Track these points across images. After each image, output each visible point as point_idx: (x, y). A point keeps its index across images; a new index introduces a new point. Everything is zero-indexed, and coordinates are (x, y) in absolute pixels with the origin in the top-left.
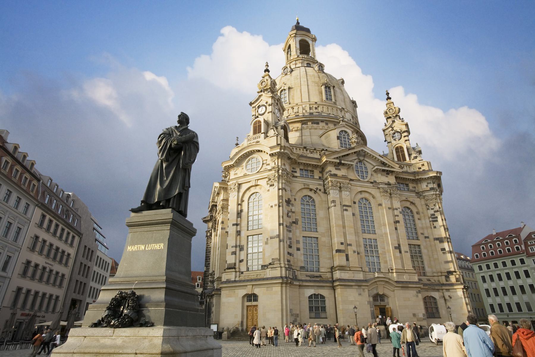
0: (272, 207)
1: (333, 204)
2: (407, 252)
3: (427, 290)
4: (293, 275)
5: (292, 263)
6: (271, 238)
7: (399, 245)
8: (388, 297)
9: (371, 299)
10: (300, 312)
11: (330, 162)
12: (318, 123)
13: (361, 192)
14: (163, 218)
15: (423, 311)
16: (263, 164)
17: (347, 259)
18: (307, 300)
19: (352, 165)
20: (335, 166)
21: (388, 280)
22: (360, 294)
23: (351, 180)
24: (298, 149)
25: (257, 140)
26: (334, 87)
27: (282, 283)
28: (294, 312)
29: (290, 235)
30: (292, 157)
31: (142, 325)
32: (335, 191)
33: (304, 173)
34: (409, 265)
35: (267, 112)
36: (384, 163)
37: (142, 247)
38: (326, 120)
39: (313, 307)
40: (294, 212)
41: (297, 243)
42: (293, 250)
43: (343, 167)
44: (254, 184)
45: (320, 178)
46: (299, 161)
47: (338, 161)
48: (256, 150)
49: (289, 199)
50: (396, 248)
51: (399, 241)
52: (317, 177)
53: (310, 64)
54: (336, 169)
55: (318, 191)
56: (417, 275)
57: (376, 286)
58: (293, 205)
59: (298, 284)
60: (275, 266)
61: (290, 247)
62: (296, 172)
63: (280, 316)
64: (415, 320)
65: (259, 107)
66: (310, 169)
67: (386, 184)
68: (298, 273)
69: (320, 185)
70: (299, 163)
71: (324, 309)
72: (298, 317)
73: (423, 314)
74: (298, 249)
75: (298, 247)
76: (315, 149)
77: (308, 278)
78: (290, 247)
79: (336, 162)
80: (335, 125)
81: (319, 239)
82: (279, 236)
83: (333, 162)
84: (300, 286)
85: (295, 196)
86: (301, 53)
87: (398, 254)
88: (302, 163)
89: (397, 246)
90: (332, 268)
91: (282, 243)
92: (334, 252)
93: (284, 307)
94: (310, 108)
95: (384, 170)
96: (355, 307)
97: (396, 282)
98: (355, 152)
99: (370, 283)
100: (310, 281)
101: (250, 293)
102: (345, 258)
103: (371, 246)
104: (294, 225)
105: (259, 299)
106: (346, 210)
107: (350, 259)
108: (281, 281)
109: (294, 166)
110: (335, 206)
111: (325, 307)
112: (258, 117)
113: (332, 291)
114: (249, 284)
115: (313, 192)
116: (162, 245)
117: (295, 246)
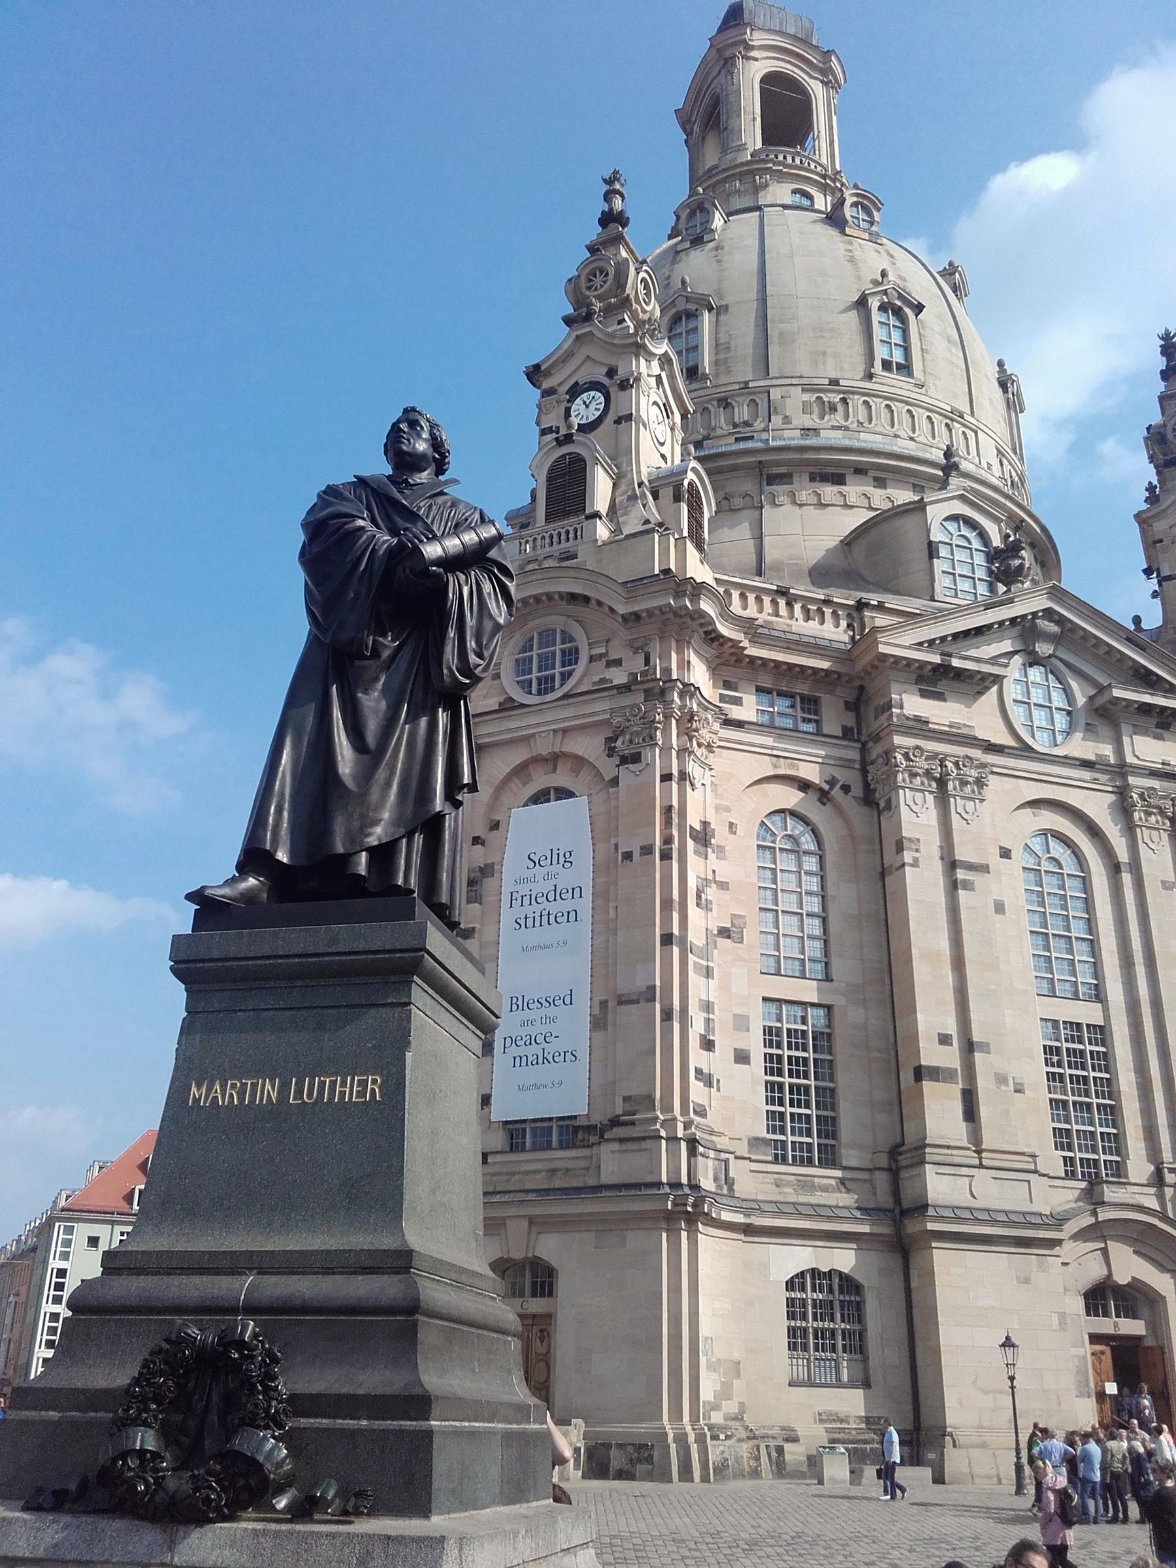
0: (628, 856)
1: (908, 857)
4: (716, 1179)
6: (622, 1001)
9: (1079, 1304)
11: (898, 660)
12: (839, 480)
13: (1035, 804)
16: (592, 659)
17: (971, 1113)
19: (998, 679)
20: (919, 680)
22: (1027, 1281)
23: (992, 748)
24: (751, 597)
25: (564, 545)
26: (919, 308)
30: (724, 629)
32: (919, 795)
33: (781, 705)
35: (611, 417)
36: (1149, 672)
38: (880, 467)
40: (723, 886)
42: (719, 1062)
43: (956, 684)
44: (545, 753)
45: (847, 733)
46: (753, 651)
47: (936, 659)
48: (561, 595)
49: (705, 824)
52: (832, 727)
53: (810, 197)
54: (924, 694)
55: (836, 792)
58: (720, 850)
59: (739, 1218)
60: (634, 1132)
61: (708, 1045)
62: (737, 701)
65: (575, 392)
66: (802, 688)
67: (1153, 773)
69: (845, 764)
70: (753, 659)
74: (742, 1057)
75: (740, 1046)
76: (827, 602)
79: (923, 664)
80: (917, 488)
83: (910, 662)
85: (727, 810)
86: (765, 142)
88: (765, 662)
90: (894, 1152)
92: (907, 1077)
94: (806, 408)
95: (1146, 709)
96: (1008, 1343)
98: (1013, 621)
101: (518, 1254)
102: (957, 1107)
104: (723, 942)
105: (563, 1284)
106: (968, 886)
107: (985, 1112)
109: (730, 674)
110: (915, 864)
111: (862, 1334)
112: (569, 439)
114: (513, 1211)
115: (813, 796)
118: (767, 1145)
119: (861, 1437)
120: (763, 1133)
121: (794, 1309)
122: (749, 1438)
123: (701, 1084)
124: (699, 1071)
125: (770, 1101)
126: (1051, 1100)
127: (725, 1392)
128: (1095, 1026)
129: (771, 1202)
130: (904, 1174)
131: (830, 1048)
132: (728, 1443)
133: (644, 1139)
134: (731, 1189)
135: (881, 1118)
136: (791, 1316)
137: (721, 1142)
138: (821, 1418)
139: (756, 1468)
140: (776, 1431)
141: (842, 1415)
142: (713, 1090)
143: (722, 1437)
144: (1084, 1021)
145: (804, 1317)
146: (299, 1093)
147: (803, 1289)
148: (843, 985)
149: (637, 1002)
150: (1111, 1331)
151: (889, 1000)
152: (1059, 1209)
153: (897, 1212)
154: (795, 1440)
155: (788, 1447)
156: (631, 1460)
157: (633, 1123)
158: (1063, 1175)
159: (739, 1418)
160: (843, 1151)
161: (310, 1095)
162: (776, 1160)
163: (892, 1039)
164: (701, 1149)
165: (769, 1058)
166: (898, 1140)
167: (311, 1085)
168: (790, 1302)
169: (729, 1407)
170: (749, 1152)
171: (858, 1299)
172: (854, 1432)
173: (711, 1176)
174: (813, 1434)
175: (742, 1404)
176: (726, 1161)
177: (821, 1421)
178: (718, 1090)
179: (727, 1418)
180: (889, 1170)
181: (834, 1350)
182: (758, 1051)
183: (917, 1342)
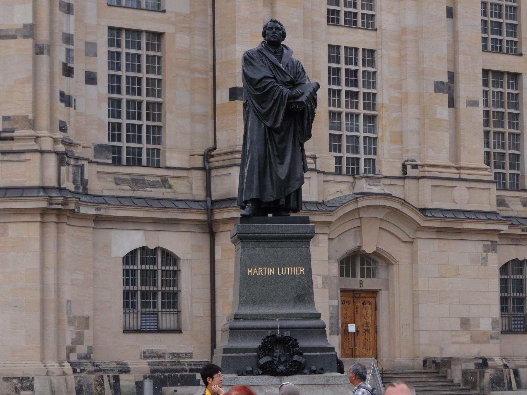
2: (473, 103)
3: (516, 239)
4: (74, 182)
5: (71, 134)
7: (452, 76)
8: (388, 262)
9: (335, 269)
10: (95, 309)
14: (301, 231)
15: (496, 311)
18: (120, 267)
21: (397, 206)
27: (43, 212)
28: (77, 311)
29: (68, 24)
31: (314, 372)
34: (474, 153)
37: (271, 271)
39: (134, 294)
41: (87, 55)
42: (75, 86)
50: (439, 87)
51: (454, 61)
56: (494, 187)
57: (357, 223)
59: (92, 211)
60: (15, 146)
61: (68, 71)
63: (36, 326)
64: (466, 337)
68: (90, 171)
71: (172, 300)
72: (87, 327)
73: (494, 321)
74: (91, 79)
75: (90, 68)
77: (126, 191)
78: (68, 71)
81: (167, 39)
82: (30, 31)
84: (97, 219)
87: (443, 112)
89: (445, 79)
90: (208, 156)
91: (44, 58)
92: (223, 95)
93: (51, 295)
97: (423, 210)
99: (340, 213)
100: (133, 202)
103: (352, 74)
108: (43, 204)
111: (176, 294)
113: (204, 240)
116: (302, 270)
117: (80, 69)
118: (109, 151)
119: (174, 367)
120: (105, 140)
121: (129, 277)
122: (96, 371)
123: (63, 105)
124: (62, 94)
125: (112, 114)
126: (330, 112)
127: (79, 340)
128: (369, 50)
129: (117, 197)
130: (214, 173)
131: (159, 69)
132: (82, 375)
133: (23, 152)
134: (85, 189)
135: (199, 127)
136: (126, 282)
137: (78, 152)
138: (145, 355)
139: (101, 391)
140: (113, 366)
141: (160, 353)
142: (72, 109)
143: (78, 370)
144: (361, 46)
145: (134, 283)
146: (280, 272)
147: (134, 263)
148: (174, 15)
149: (14, 37)
150: (357, 287)
151: (210, 29)
152: (330, 198)
153: (209, 203)
154: (127, 371)
155: (122, 376)
156: (16, 389)
157: (12, 139)
158: (333, 170)
159: (87, 357)
160: (168, 154)
161: (284, 273)
162: (114, 164)
163: (211, 62)
164: (67, 159)
165: (111, 77)
166: (211, 145)
167: (284, 270)
168: (126, 272)
169: (82, 350)
170: (95, 157)
171: (175, 268)
172: (169, 364)
173: (71, 179)
174: (141, 367)
175: (90, 348)
176: (82, 167)
177: (145, 357)
178: (75, 108)
179: (80, 357)
180: (204, 169)
181: (155, 306)
182: (103, 72)
183: (217, 299)
